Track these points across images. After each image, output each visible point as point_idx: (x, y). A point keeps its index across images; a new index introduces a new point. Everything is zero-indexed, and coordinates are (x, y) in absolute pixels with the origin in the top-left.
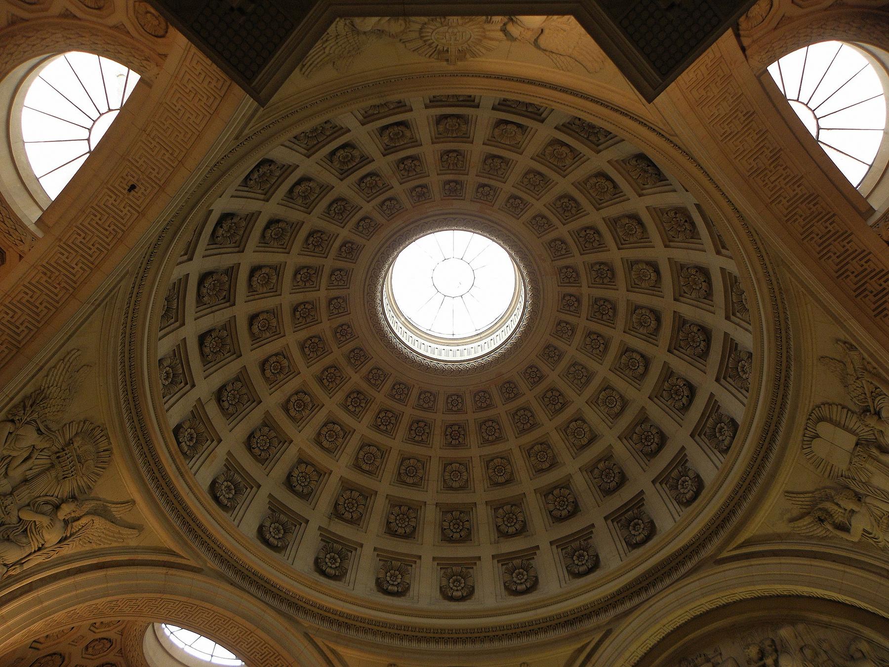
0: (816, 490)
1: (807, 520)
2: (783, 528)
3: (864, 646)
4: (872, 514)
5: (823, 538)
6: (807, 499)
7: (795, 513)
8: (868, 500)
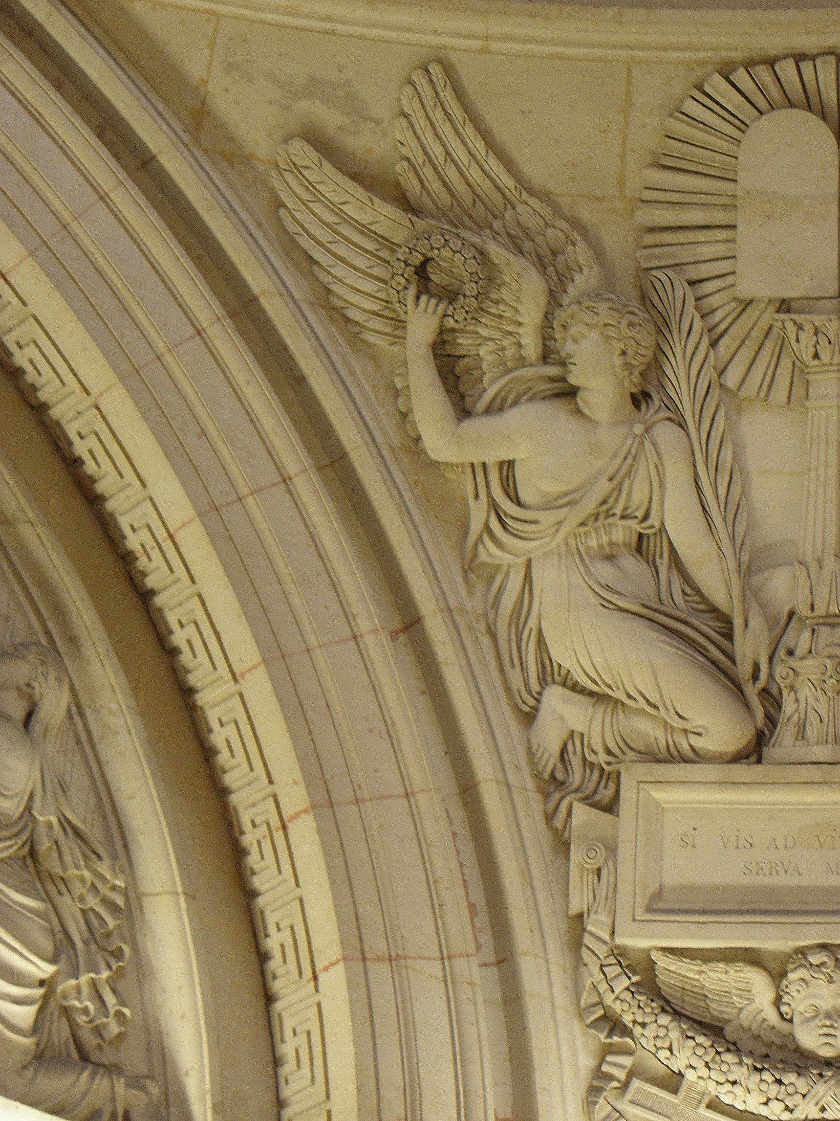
0: (544, 196)
1: (384, 216)
2: (251, 115)
3: (54, 704)
4: (619, 480)
5: (337, 315)
6: (474, 173)
7: (369, 143)
8: (666, 434)
